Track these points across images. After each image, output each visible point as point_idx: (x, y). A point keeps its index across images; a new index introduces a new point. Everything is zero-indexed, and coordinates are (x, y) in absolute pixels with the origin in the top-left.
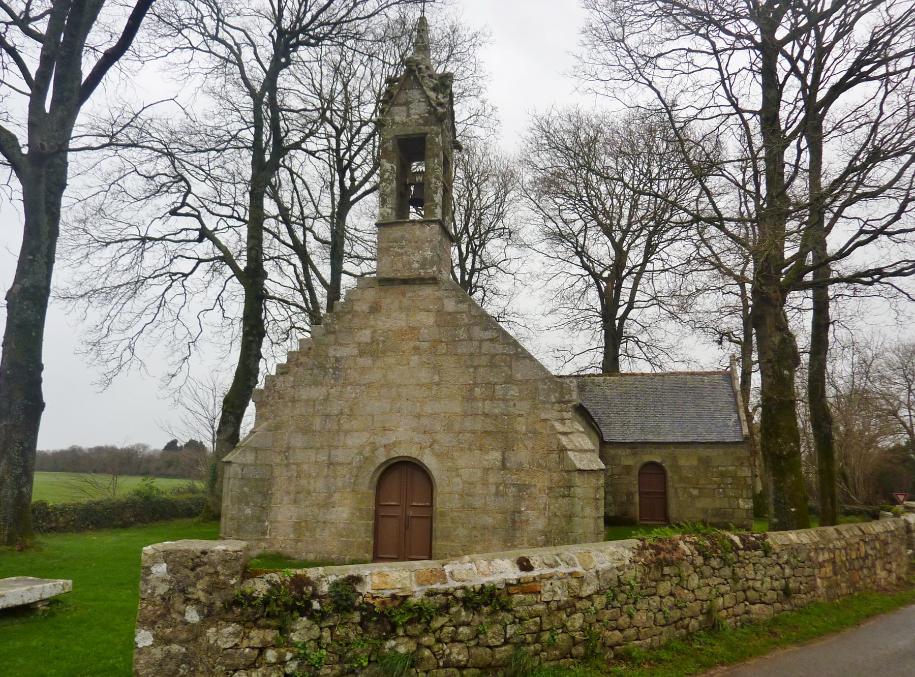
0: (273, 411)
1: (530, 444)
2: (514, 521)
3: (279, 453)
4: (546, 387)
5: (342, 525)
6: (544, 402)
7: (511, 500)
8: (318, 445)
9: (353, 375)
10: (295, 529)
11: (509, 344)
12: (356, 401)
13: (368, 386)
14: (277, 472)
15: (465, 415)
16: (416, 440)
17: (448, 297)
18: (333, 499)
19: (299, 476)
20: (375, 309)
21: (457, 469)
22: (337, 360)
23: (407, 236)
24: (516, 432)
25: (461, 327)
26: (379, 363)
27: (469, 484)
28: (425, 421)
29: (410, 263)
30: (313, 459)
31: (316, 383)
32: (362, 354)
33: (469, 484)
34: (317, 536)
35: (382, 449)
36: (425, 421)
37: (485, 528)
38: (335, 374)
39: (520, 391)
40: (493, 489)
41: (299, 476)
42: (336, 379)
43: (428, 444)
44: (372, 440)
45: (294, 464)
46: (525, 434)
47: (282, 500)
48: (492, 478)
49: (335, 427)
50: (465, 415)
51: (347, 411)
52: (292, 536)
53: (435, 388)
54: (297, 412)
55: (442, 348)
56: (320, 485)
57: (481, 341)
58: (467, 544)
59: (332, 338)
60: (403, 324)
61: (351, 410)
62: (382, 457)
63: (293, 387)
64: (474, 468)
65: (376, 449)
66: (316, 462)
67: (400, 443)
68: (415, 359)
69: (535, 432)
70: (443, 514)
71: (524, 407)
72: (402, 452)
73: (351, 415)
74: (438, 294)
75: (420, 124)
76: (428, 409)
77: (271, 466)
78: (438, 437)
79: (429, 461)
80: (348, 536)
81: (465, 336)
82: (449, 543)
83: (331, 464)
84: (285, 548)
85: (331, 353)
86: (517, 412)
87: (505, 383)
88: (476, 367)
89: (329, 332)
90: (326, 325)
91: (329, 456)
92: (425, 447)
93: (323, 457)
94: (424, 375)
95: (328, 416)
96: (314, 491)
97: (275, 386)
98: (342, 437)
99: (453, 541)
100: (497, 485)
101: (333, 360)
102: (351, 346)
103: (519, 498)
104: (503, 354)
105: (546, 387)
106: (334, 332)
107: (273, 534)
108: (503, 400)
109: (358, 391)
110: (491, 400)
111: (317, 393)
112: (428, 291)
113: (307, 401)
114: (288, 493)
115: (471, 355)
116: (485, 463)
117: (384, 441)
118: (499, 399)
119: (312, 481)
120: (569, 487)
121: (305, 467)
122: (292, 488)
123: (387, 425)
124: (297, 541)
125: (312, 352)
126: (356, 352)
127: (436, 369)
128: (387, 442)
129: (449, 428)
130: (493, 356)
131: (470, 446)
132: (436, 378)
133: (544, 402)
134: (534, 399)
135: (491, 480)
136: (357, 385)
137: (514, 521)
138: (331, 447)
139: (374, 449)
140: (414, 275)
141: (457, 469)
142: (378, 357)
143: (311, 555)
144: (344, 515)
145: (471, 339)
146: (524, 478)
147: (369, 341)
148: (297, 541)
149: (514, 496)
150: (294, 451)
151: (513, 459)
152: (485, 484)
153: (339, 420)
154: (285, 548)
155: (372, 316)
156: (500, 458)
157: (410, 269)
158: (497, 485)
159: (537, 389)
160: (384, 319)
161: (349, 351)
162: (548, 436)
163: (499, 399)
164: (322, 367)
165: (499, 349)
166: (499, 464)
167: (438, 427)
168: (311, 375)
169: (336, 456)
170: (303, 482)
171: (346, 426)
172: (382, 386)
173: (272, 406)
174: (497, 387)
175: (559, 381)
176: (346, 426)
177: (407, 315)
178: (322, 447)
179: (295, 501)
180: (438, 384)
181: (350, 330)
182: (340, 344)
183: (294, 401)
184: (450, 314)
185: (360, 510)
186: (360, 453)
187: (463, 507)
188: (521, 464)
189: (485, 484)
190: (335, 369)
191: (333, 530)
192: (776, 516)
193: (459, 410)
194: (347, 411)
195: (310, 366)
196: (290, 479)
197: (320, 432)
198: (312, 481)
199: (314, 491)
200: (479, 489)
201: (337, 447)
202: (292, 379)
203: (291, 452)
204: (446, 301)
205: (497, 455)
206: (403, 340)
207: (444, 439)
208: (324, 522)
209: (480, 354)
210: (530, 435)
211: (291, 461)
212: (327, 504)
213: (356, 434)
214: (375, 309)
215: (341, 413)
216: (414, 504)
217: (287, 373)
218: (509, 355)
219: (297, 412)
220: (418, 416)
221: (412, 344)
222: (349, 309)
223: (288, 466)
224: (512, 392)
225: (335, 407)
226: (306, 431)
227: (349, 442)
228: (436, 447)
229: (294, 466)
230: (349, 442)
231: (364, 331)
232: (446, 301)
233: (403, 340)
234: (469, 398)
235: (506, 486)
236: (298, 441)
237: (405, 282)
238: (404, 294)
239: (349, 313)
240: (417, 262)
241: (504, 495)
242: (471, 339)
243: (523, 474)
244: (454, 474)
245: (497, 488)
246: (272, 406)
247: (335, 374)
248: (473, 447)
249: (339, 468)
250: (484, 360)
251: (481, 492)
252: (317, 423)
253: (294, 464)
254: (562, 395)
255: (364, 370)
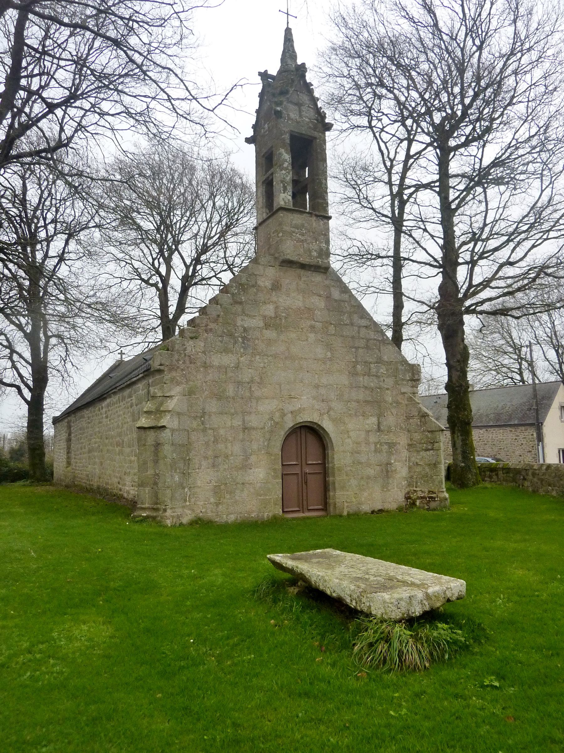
0: (185, 376)
1: (394, 411)
2: (387, 472)
3: (195, 418)
4: (403, 368)
5: (259, 485)
6: (403, 380)
7: (385, 455)
8: (233, 411)
9: (261, 346)
10: (215, 493)
11: (378, 332)
12: (264, 370)
13: (275, 356)
14: (193, 437)
15: (351, 387)
16: (317, 407)
17: (333, 286)
18: (249, 462)
19: (216, 441)
20: (276, 287)
21: (348, 432)
22: (245, 330)
23: (306, 225)
24: (386, 402)
25: (345, 313)
26: (282, 337)
27: (357, 443)
28: (323, 391)
29: (310, 251)
30: (229, 424)
31: (226, 351)
32: (267, 326)
33: (357, 443)
34: (237, 498)
35: (290, 415)
36: (323, 391)
37: (369, 478)
38: (243, 343)
39: (387, 370)
40: (373, 447)
41: (216, 441)
42: (245, 348)
43: (326, 411)
44: (280, 407)
45: (210, 429)
46: (391, 404)
47: (201, 465)
48: (373, 438)
49: (248, 394)
50: (351, 387)
51: (257, 379)
52: (212, 500)
53: (328, 363)
54: (210, 377)
55: (332, 329)
56: (237, 449)
57: (359, 327)
58: (357, 492)
59: (239, 308)
60: (301, 304)
61: (261, 378)
62: (289, 423)
63: (204, 352)
64: (359, 430)
65: (285, 415)
66: (232, 427)
67: (304, 409)
68: (312, 336)
69: (398, 403)
70: (339, 470)
71: (390, 382)
72: (306, 417)
73: (261, 383)
74: (327, 282)
75: (310, 128)
76: (324, 381)
77: (188, 431)
78: (333, 405)
79: (327, 425)
80: (266, 495)
81: (348, 322)
82: (345, 493)
83: (246, 429)
84: (206, 512)
85: (239, 323)
86: (386, 386)
87: (377, 363)
88: (357, 348)
89: (236, 302)
90: (233, 295)
91: (244, 421)
92: (324, 414)
93: (237, 422)
94: (320, 351)
95: (239, 383)
96: (232, 455)
97: (185, 350)
98: (254, 404)
99: (348, 491)
100: (376, 444)
101: (241, 329)
102: (257, 318)
103: (390, 453)
104: (375, 339)
105: (403, 368)
106: (241, 303)
107: (193, 500)
108: (376, 376)
109: (266, 361)
110: (369, 376)
111: (228, 360)
112: (318, 278)
113: (220, 367)
114: (206, 458)
115: (353, 337)
116: (367, 426)
117: (291, 408)
118: (374, 375)
119: (229, 445)
120: (433, 443)
121: (222, 432)
122: (210, 453)
123: (293, 394)
124: (217, 504)
125: (221, 320)
126: (261, 324)
127: (329, 347)
128: (294, 409)
129: (340, 397)
130: (368, 340)
131: (356, 413)
132: (329, 354)
133: (403, 380)
134: (396, 377)
135: (371, 440)
136: (265, 355)
137: (387, 472)
138: (244, 413)
139: (283, 415)
140: (313, 262)
141: (348, 432)
142: (281, 331)
143: (232, 516)
144: (261, 476)
145: (352, 324)
146: (392, 438)
147: (273, 315)
148: (217, 504)
149: (386, 452)
150: (210, 416)
151: (385, 423)
152: (368, 443)
153: (250, 388)
154: (206, 512)
155: (274, 293)
156: (376, 422)
157: (310, 256)
158: (376, 444)
159: (397, 369)
160: (285, 297)
161: (256, 322)
162: (406, 405)
163: (374, 375)
164: (231, 335)
165: (372, 335)
166: (376, 427)
167: (332, 396)
168: (221, 342)
169: (250, 421)
170: (221, 446)
171: (257, 393)
172: (286, 358)
173: (182, 370)
174: (372, 366)
175: (410, 364)
176: (257, 393)
177: (303, 297)
178: (236, 413)
179: (214, 466)
180: (331, 359)
181: (256, 303)
182: (247, 315)
183: (206, 366)
184: (336, 301)
185: (275, 470)
186: (271, 419)
187: (354, 463)
188: (390, 427)
189: (368, 443)
190: (244, 338)
191: (252, 490)
192: (463, 462)
193: (347, 383)
194: (257, 379)
195: (219, 333)
196: (207, 444)
197: (233, 398)
198: (229, 445)
199: (232, 455)
200: (363, 448)
201: (250, 413)
202: (202, 344)
203: (207, 417)
204: (332, 289)
205: (374, 420)
206: (301, 318)
207: (338, 406)
208: (243, 484)
209: (359, 338)
210: (394, 404)
211: (208, 426)
212: (245, 466)
213: (267, 401)
214: (276, 287)
215: (252, 381)
216: (310, 462)
217: (196, 338)
218: (378, 340)
219: (210, 377)
220: (317, 387)
221: (309, 323)
222: (253, 282)
223: (204, 430)
224: (382, 370)
225: (246, 375)
226: (220, 397)
227: (261, 408)
228: (332, 413)
229: (210, 432)
230: (261, 408)
231: (268, 306)
232: (332, 289)
233: (301, 318)
234: (354, 374)
235: (381, 445)
236: (213, 406)
237: (303, 266)
238: (300, 277)
239: (253, 286)
240: (316, 251)
241: (380, 451)
242: (352, 324)
243: (391, 435)
244: (346, 436)
245: (376, 446)
246: (182, 370)
247: (243, 343)
248: (358, 414)
249: (254, 433)
250: (362, 343)
251: (365, 449)
252: (231, 390)
253: (210, 429)
254: (413, 374)
255: (270, 342)
